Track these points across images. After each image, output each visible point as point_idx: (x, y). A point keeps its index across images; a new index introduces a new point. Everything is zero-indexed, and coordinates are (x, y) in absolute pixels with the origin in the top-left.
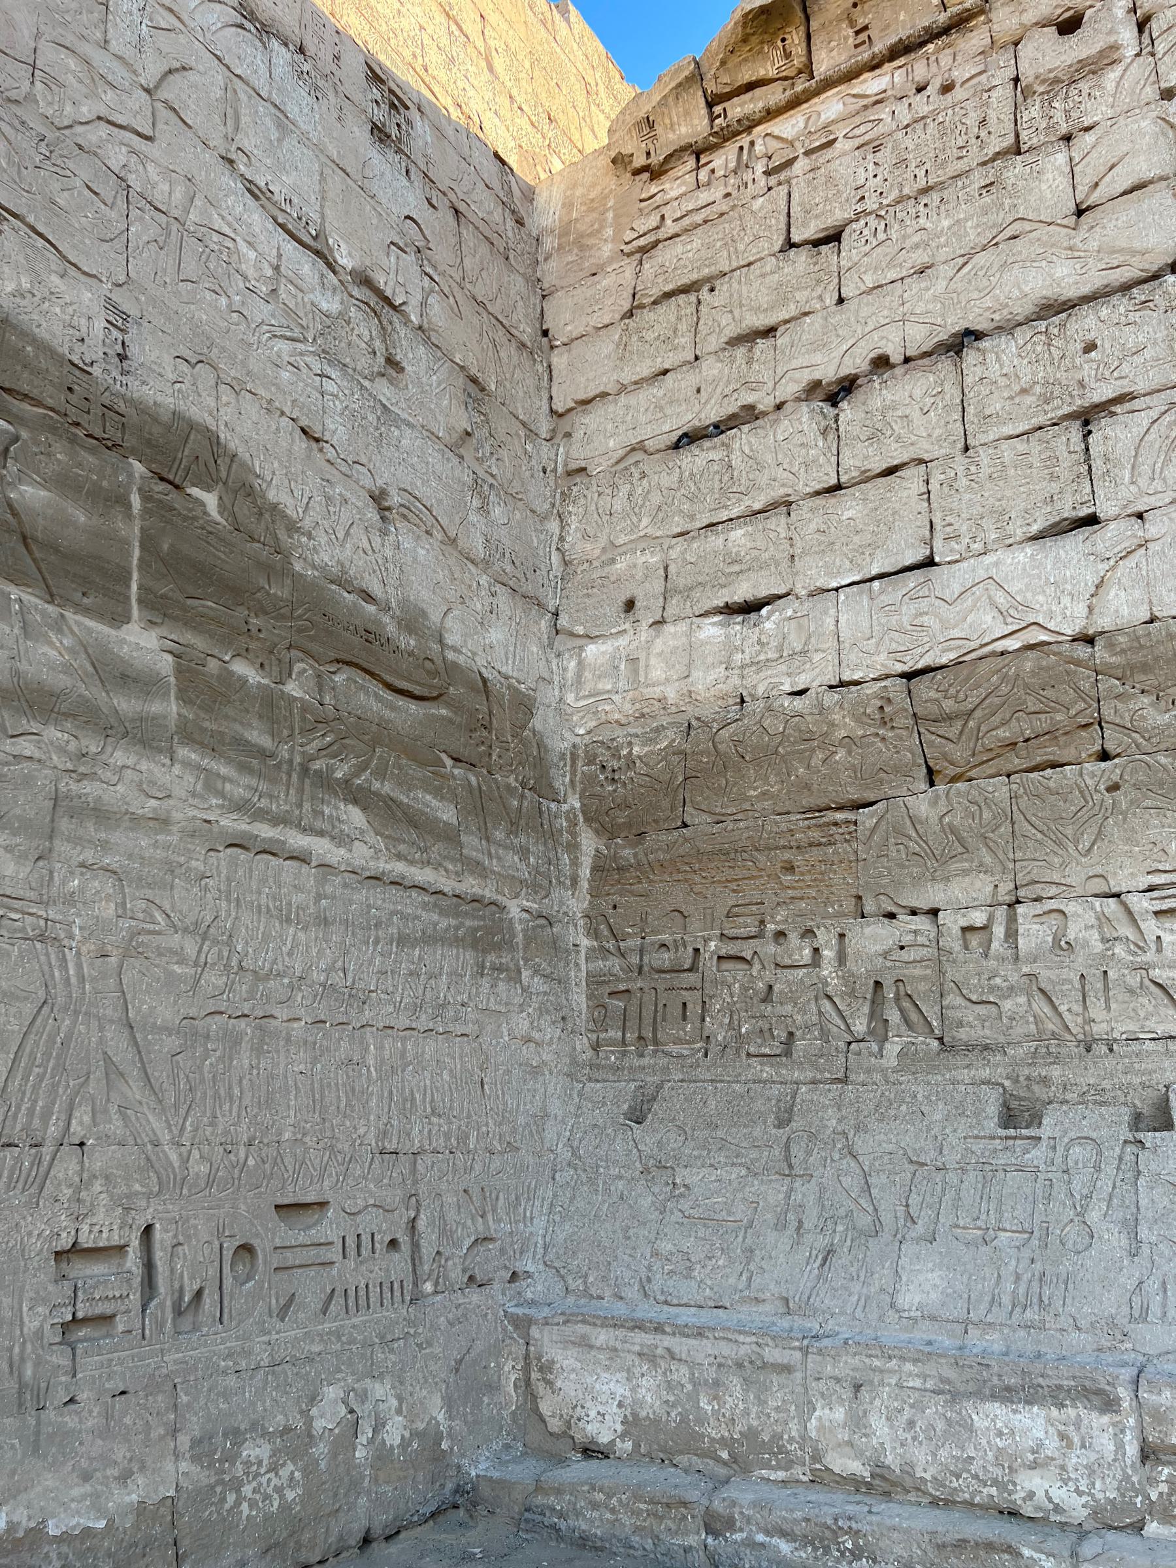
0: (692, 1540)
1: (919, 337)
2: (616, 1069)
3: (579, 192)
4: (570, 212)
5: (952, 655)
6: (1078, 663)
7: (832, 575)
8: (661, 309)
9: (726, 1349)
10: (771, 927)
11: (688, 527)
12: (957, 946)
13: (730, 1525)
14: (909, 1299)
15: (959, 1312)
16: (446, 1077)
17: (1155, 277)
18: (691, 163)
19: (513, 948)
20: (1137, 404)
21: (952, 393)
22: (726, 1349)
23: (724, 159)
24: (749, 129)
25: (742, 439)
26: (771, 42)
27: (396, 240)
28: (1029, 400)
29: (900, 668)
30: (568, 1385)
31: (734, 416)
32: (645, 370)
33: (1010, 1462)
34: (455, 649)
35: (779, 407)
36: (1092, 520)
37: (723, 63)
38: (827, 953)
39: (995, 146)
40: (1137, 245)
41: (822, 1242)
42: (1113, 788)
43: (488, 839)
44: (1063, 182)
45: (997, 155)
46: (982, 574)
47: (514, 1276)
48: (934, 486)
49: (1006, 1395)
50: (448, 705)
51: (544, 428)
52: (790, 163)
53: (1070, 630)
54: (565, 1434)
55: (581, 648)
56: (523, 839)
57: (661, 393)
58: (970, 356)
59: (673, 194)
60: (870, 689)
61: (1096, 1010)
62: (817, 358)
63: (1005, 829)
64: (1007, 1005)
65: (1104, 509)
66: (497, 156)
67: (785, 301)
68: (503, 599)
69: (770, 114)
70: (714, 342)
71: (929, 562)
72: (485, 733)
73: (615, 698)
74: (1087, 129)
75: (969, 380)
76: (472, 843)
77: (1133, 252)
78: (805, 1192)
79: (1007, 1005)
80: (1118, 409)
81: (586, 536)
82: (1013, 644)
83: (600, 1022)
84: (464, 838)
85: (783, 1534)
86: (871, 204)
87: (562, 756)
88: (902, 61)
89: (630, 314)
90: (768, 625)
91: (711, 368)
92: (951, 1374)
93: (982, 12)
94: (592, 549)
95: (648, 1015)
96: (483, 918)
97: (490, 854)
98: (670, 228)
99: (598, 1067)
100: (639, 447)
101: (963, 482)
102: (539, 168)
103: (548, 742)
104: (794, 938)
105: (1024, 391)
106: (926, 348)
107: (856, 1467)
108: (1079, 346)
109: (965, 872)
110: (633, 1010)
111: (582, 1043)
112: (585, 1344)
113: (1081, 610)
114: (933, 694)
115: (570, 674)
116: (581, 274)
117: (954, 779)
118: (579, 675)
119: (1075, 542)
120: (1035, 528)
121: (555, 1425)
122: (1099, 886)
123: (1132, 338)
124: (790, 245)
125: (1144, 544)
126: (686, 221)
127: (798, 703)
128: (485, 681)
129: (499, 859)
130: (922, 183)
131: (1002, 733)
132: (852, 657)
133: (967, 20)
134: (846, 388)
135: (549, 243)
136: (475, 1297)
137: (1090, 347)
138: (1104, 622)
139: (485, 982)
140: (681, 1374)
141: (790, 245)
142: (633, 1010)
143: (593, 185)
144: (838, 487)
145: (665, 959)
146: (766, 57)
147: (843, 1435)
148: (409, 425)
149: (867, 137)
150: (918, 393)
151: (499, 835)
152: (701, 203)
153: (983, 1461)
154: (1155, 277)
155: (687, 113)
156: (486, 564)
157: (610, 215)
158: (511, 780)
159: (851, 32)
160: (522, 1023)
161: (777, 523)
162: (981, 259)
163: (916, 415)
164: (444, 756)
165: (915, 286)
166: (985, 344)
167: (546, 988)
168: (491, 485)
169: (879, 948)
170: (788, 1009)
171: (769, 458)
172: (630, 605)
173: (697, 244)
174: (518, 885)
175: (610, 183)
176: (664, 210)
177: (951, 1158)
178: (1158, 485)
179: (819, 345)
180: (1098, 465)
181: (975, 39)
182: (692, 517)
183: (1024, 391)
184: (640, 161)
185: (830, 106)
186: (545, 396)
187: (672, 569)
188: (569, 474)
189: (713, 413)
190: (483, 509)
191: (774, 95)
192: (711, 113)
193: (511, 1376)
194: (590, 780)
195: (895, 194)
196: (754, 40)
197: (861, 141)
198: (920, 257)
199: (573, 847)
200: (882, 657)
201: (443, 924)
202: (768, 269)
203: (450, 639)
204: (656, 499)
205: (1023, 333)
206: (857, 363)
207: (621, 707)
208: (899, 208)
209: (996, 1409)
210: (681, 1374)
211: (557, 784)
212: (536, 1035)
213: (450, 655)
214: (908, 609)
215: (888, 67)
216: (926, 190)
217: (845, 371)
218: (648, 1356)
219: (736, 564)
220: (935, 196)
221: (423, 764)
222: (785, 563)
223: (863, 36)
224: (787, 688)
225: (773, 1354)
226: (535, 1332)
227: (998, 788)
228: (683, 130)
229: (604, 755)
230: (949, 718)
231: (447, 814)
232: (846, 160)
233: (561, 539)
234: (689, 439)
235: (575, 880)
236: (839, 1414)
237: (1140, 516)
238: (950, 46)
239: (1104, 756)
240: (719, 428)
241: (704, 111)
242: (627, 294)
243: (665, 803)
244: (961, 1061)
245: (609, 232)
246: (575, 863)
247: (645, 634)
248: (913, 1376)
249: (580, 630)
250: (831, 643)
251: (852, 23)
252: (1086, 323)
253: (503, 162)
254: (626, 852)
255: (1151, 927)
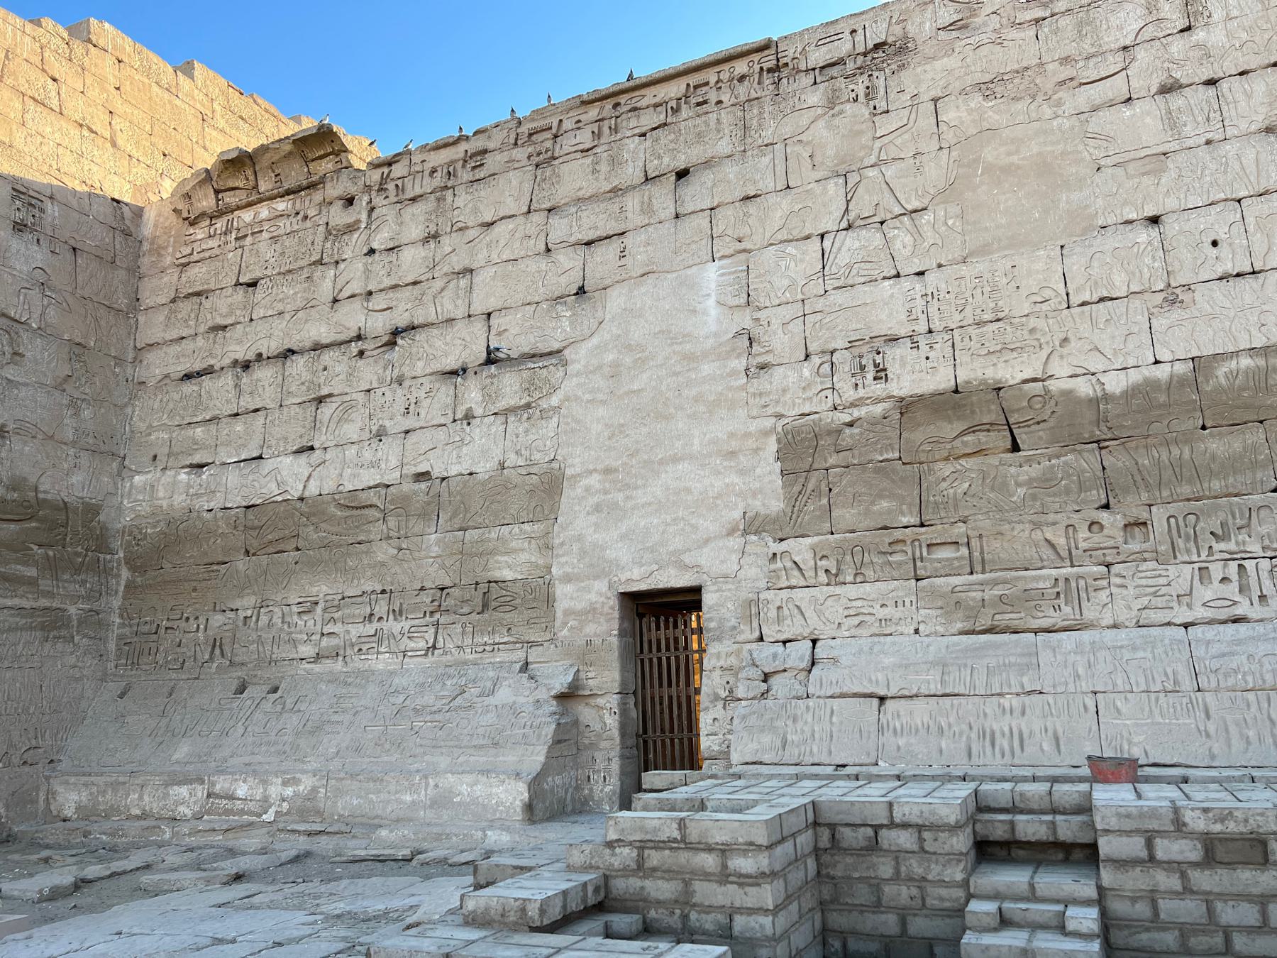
0: (78, 840)
1: (271, 346)
2: (122, 676)
3: (162, 220)
4: (156, 231)
5: (260, 501)
6: (296, 510)
7: (230, 457)
8: (186, 302)
9: (108, 779)
10: (185, 615)
11: (181, 423)
12: (241, 624)
13: (90, 833)
14: (174, 758)
15: (185, 760)
16: (18, 685)
17: (350, 341)
18: (208, 222)
19: (68, 626)
20: (333, 399)
21: (280, 378)
22: (108, 779)
23: (220, 224)
24: (232, 211)
25: (206, 380)
26: (239, 172)
27: (25, 285)
28: (304, 388)
29: (244, 504)
30: (60, 799)
31: (205, 369)
32: (175, 334)
33: (177, 803)
34: (45, 492)
35: (222, 368)
36: (312, 448)
37: (219, 176)
38: (202, 626)
39: (313, 259)
40: (347, 325)
41: (161, 740)
42: (296, 563)
43: (57, 580)
44: (330, 284)
45: (314, 263)
46: (275, 466)
47: (52, 761)
48: (268, 422)
49: (179, 783)
50: (38, 521)
51: (130, 357)
52: (246, 236)
53: (297, 495)
54: (58, 816)
55: (133, 477)
56: (83, 576)
57: (179, 349)
58: (288, 363)
59: (199, 237)
60: (233, 512)
61: (275, 650)
62: (238, 348)
63: (263, 577)
64: (251, 647)
65: (316, 445)
66: (113, 199)
67: (231, 313)
68: (85, 459)
69: (239, 208)
70: (202, 329)
71: (260, 457)
72: (62, 529)
73: (144, 504)
74: (344, 260)
75: (287, 373)
76: (45, 584)
77: (345, 327)
78: (165, 721)
79: (251, 647)
80: (328, 400)
81: (141, 419)
82: (279, 498)
83: (119, 657)
84: (40, 582)
85: (104, 834)
86: (269, 272)
87: (118, 531)
88: (291, 197)
89: (173, 301)
90: (204, 477)
91: (200, 342)
92: (166, 778)
93: (320, 183)
94: (142, 426)
95: (136, 653)
96: (50, 616)
97: (58, 587)
98: (195, 257)
99: (115, 675)
100: (167, 376)
101: (277, 422)
102: (150, 194)
103: (109, 526)
104: (192, 620)
105: (303, 384)
106: (275, 354)
107: (138, 812)
108: (321, 367)
109: (248, 594)
110: (131, 652)
111: (110, 665)
112: (67, 783)
113: (301, 487)
114: (252, 517)
115: (127, 490)
116: (157, 271)
117: (254, 555)
118: (130, 491)
119: (303, 458)
120: (295, 448)
121: (55, 813)
122: (284, 602)
123: (338, 369)
124: (238, 284)
125: (324, 462)
126: (202, 255)
127: (209, 516)
128: (65, 503)
129: (64, 588)
130: (287, 268)
131: (270, 537)
132: (229, 497)
133: (317, 185)
134: (246, 366)
135: (146, 246)
136: (27, 769)
137: (325, 369)
138: (307, 494)
139: (48, 646)
140: (95, 789)
141: (238, 284)
142: (132, 650)
143: (167, 218)
144: (237, 414)
145: (146, 628)
146: (237, 178)
147: (136, 803)
148: (26, 385)
149: (275, 234)
150: (269, 375)
151: (66, 577)
152: (209, 246)
153: (170, 802)
154: (350, 341)
155: (206, 195)
156: (74, 444)
157: (172, 239)
158: (79, 549)
159: (273, 175)
160: (72, 660)
161: (213, 428)
162: (301, 314)
163: (267, 386)
164: (32, 546)
165: (276, 321)
166: (294, 358)
167: (91, 643)
168: (84, 400)
169: (218, 625)
170: (185, 650)
171: (214, 394)
172: (155, 457)
173: (203, 270)
174: (75, 598)
175: (173, 219)
176: (195, 245)
177: (213, 705)
178: (332, 437)
179: (240, 342)
180: (318, 423)
181: (318, 196)
182: (183, 418)
183: (303, 384)
184: (185, 215)
185: (264, 211)
186: (133, 338)
187: (173, 443)
188: (139, 383)
189: (198, 366)
190: (77, 414)
191: (240, 197)
192: (217, 197)
193: (42, 797)
194: (129, 543)
195: (277, 270)
196: (231, 170)
197: (271, 235)
198: (280, 307)
199: (118, 576)
200: (239, 498)
201: (24, 621)
202: (228, 294)
203: (42, 488)
204: (171, 405)
205: (306, 356)
206: (251, 356)
207: (145, 509)
208: (278, 277)
209: (176, 788)
210: (95, 789)
211: (112, 546)
212: (80, 664)
213: (41, 496)
214: (251, 477)
215: (287, 197)
216: (289, 271)
217: (247, 358)
218: (86, 785)
219: (196, 445)
220: (289, 277)
221: (16, 551)
222: (213, 448)
223: (278, 179)
224: (206, 508)
225: (121, 779)
226: (51, 781)
227: (264, 559)
228: (204, 203)
229: (136, 532)
230: (254, 528)
231: (31, 572)
232: (265, 243)
233: (131, 419)
234: (188, 377)
235: (116, 592)
236: (136, 796)
237: (325, 449)
238: (310, 194)
239: (298, 549)
240: (199, 374)
241: (213, 196)
242: (174, 289)
243: (156, 558)
244: (234, 669)
245: (170, 250)
246: (118, 584)
247: (158, 474)
248: (157, 781)
249: (133, 467)
250: (223, 489)
251: (274, 172)
252: (327, 357)
253: (118, 202)
254: (139, 579)
255: (295, 618)
